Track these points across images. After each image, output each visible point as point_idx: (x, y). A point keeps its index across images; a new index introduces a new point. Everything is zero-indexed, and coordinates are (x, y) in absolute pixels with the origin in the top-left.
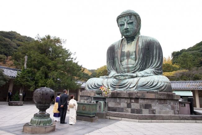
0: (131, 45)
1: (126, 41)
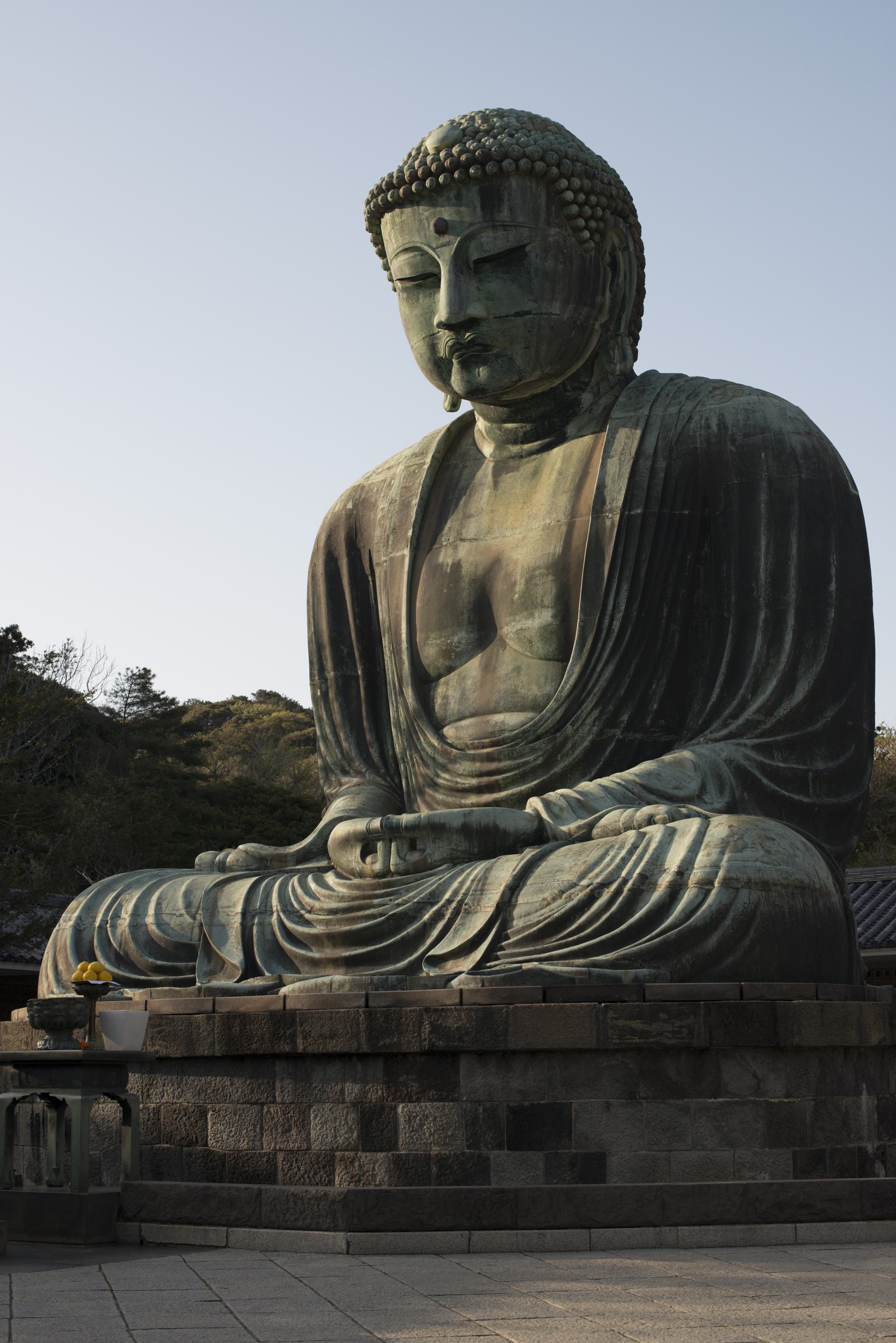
0: (527, 498)
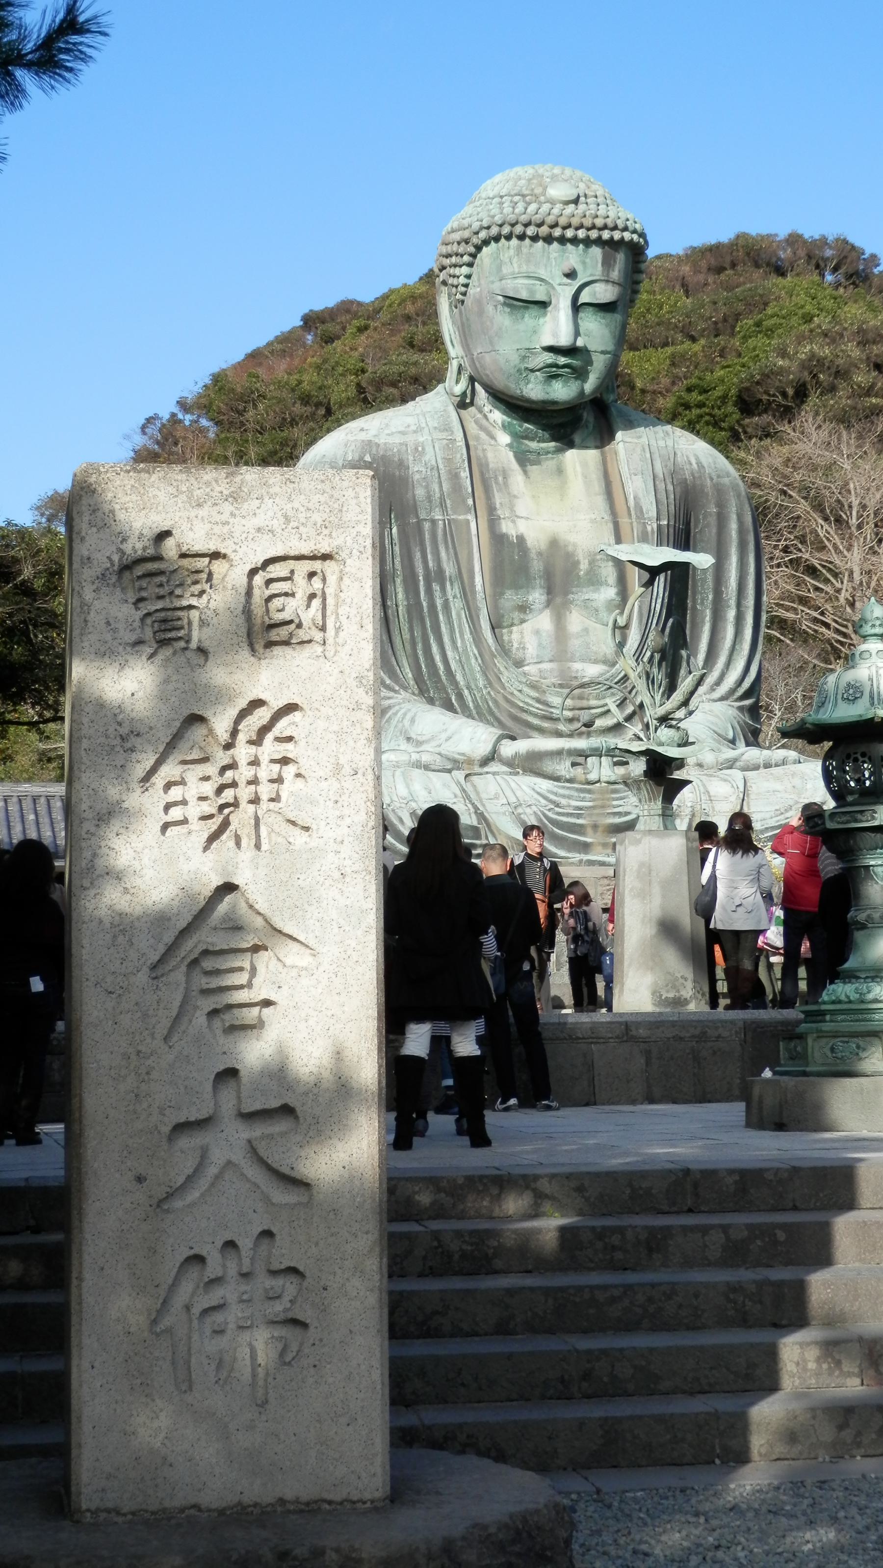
1: (505, 439)
